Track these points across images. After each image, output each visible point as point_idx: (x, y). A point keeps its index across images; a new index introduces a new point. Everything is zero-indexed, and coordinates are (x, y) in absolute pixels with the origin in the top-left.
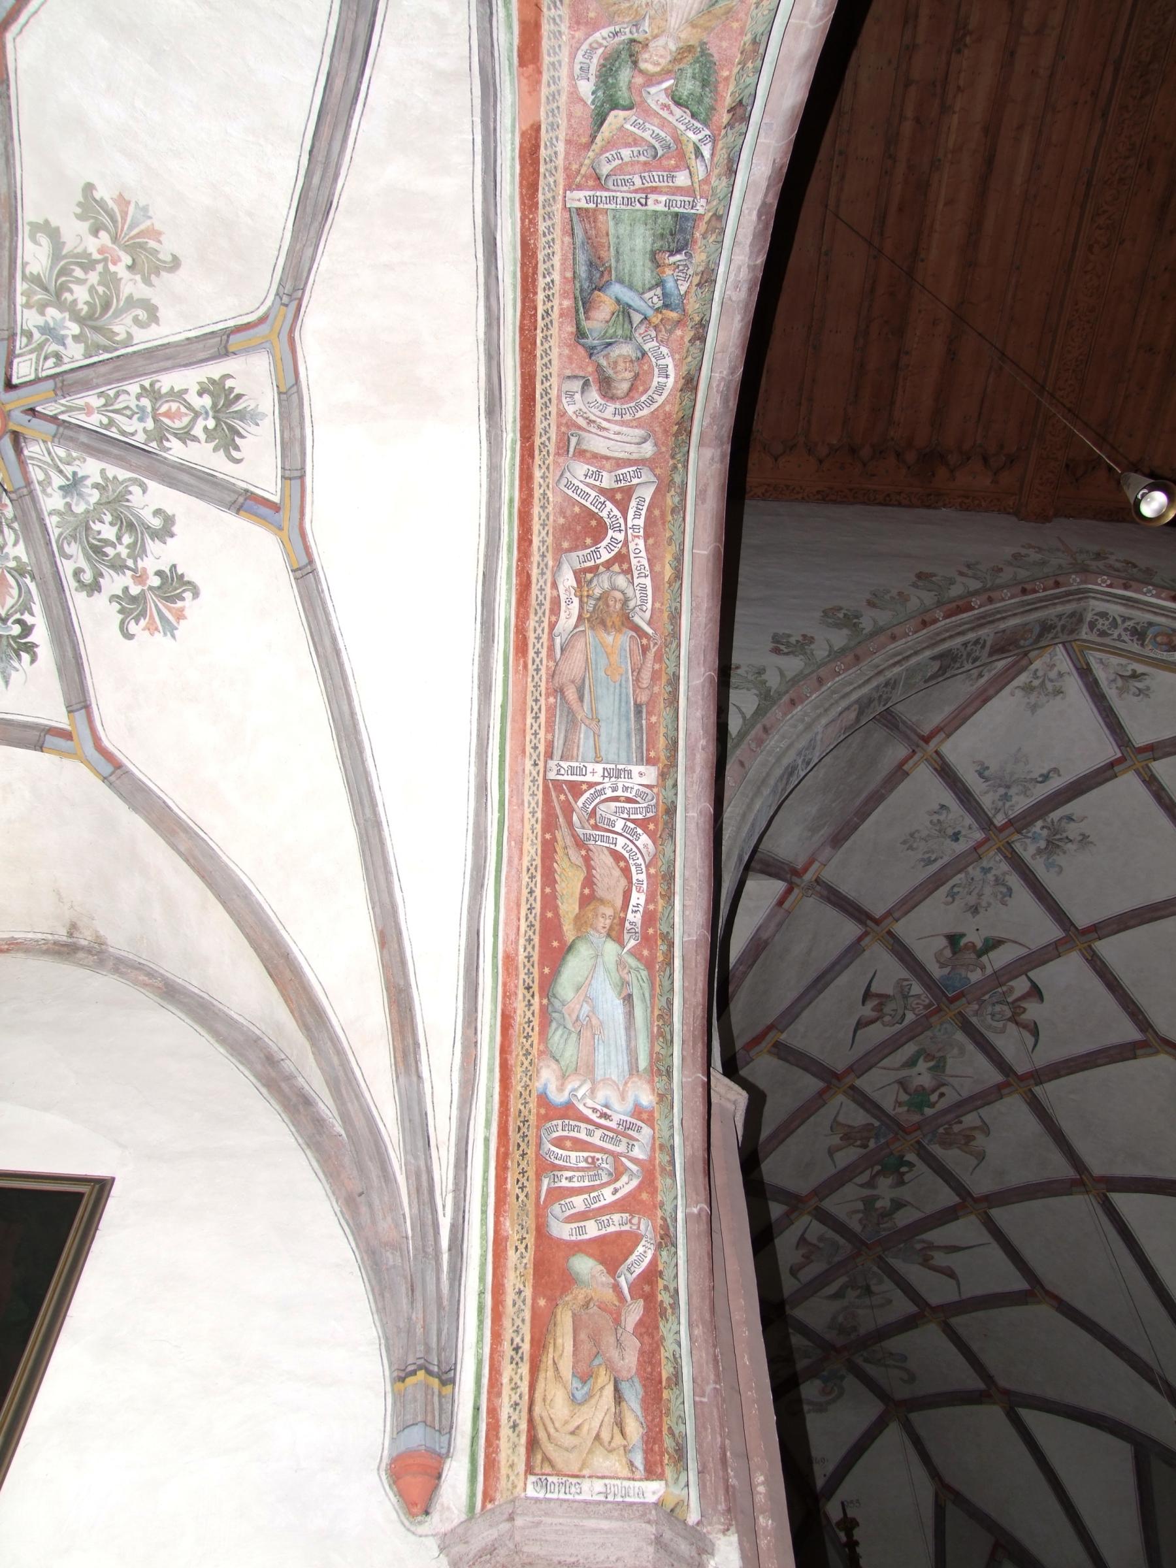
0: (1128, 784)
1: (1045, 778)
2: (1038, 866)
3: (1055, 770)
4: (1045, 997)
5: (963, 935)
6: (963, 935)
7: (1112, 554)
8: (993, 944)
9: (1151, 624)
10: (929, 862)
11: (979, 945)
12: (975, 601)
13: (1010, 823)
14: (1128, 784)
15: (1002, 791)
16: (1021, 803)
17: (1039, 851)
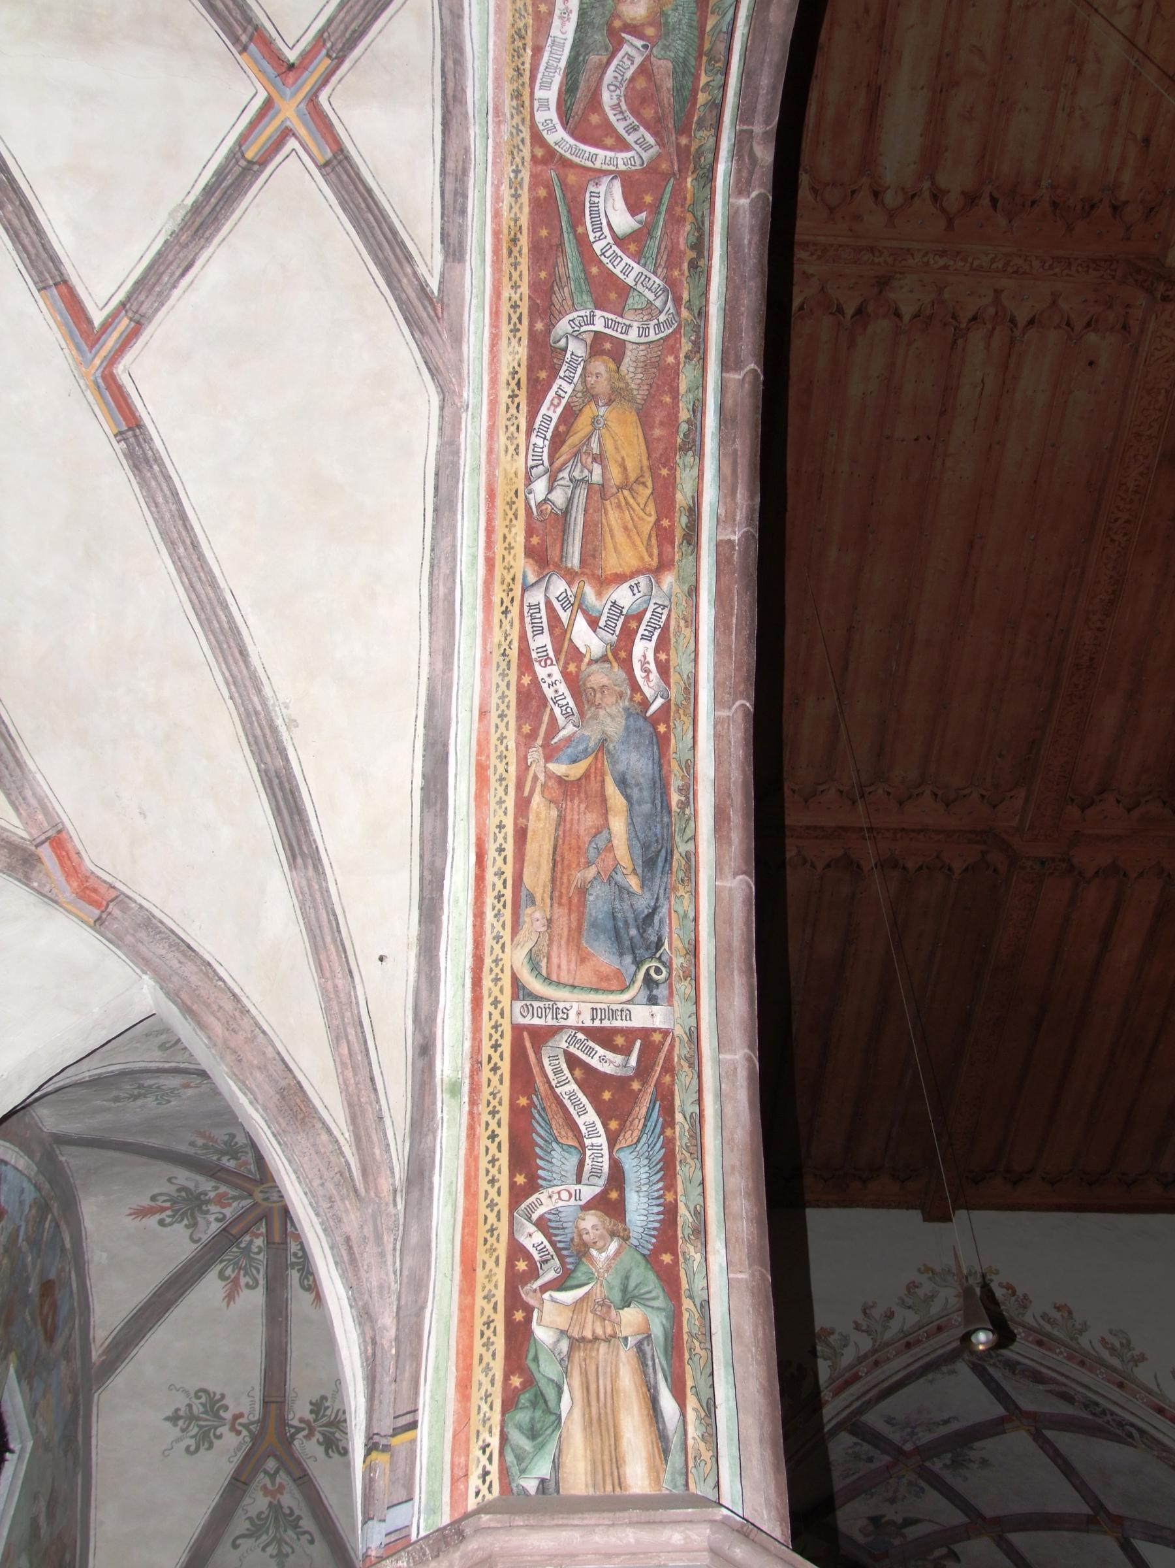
0: (1019, 1440)
1: (946, 1422)
2: (947, 1476)
3: (956, 1418)
4: (961, 1556)
5: (883, 1516)
6: (883, 1516)
7: (997, 1273)
8: (909, 1522)
9: (1018, 1363)
10: (848, 1476)
11: (900, 1521)
12: (862, 1369)
13: (918, 1450)
14: (1019, 1440)
15: (909, 1430)
16: (925, 1437)
17: (945, 1466)
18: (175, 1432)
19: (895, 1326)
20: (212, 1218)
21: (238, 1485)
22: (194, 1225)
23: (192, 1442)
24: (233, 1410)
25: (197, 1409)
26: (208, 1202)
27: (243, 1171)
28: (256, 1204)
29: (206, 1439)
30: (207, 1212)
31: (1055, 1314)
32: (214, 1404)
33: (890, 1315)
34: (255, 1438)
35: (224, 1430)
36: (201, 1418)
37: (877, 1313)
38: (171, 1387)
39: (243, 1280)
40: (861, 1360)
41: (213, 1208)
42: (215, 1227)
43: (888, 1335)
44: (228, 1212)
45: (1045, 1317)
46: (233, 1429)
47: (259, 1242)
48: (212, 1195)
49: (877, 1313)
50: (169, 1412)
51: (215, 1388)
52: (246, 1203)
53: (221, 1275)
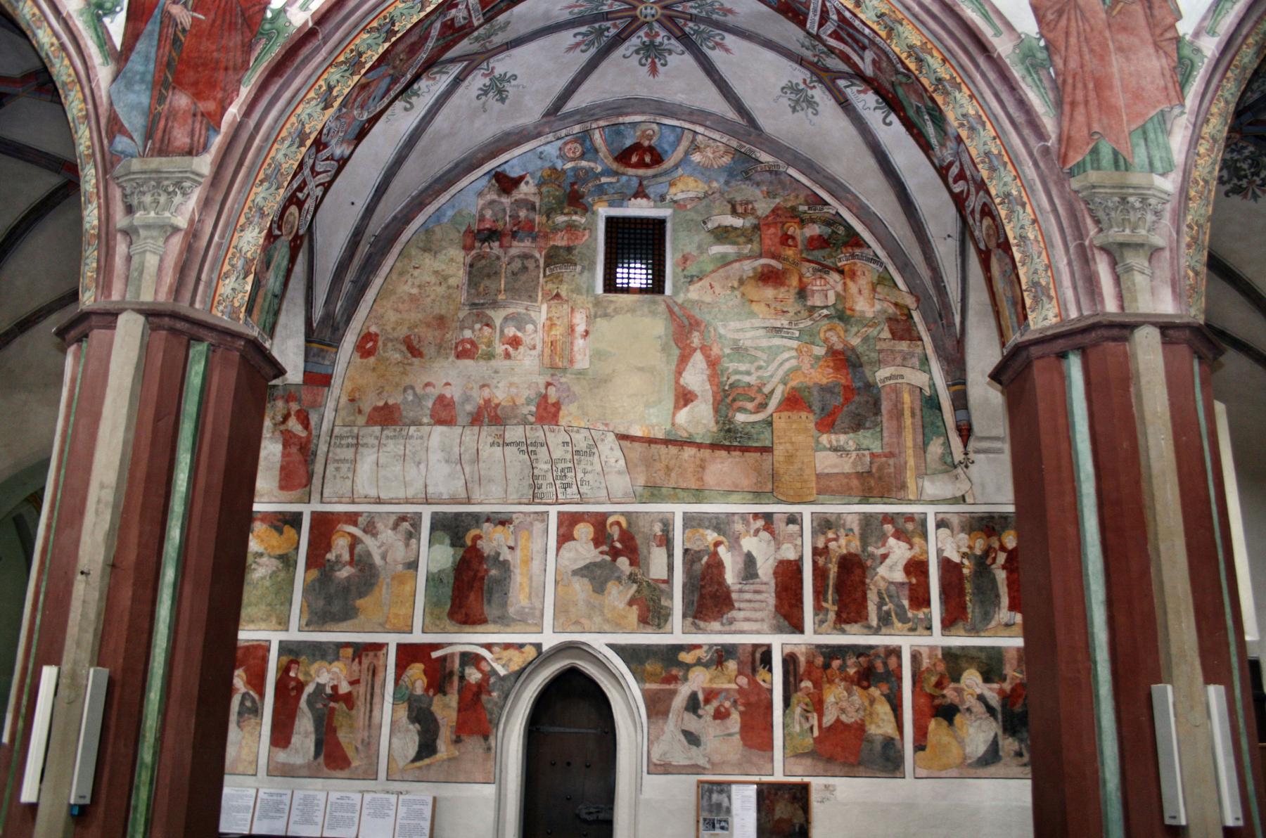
18: (801, 114)
20: (666, 42)
21: (845, 104)
22: (670, 52)
23: (810, 110)
24: (801, 82)
25: (793, 96)
26: (652, 42)
27: (622, 26)
28: (657, 21)
29: (811, 103)
30: (661, 44)
32: (792, 88)
34: (821, 81)
35: (810, 92)
36: (799, 99)
38: (776, 101)
39: (717, 39)
41: (658, 40)
42: (673, 41)
44: (663, 33)
46: (812, 88)
47: (691, 24)
48: (645, 39)
50: (790, 110)
51: (784, 83)
52: (656, 25)
53: (713, 48)
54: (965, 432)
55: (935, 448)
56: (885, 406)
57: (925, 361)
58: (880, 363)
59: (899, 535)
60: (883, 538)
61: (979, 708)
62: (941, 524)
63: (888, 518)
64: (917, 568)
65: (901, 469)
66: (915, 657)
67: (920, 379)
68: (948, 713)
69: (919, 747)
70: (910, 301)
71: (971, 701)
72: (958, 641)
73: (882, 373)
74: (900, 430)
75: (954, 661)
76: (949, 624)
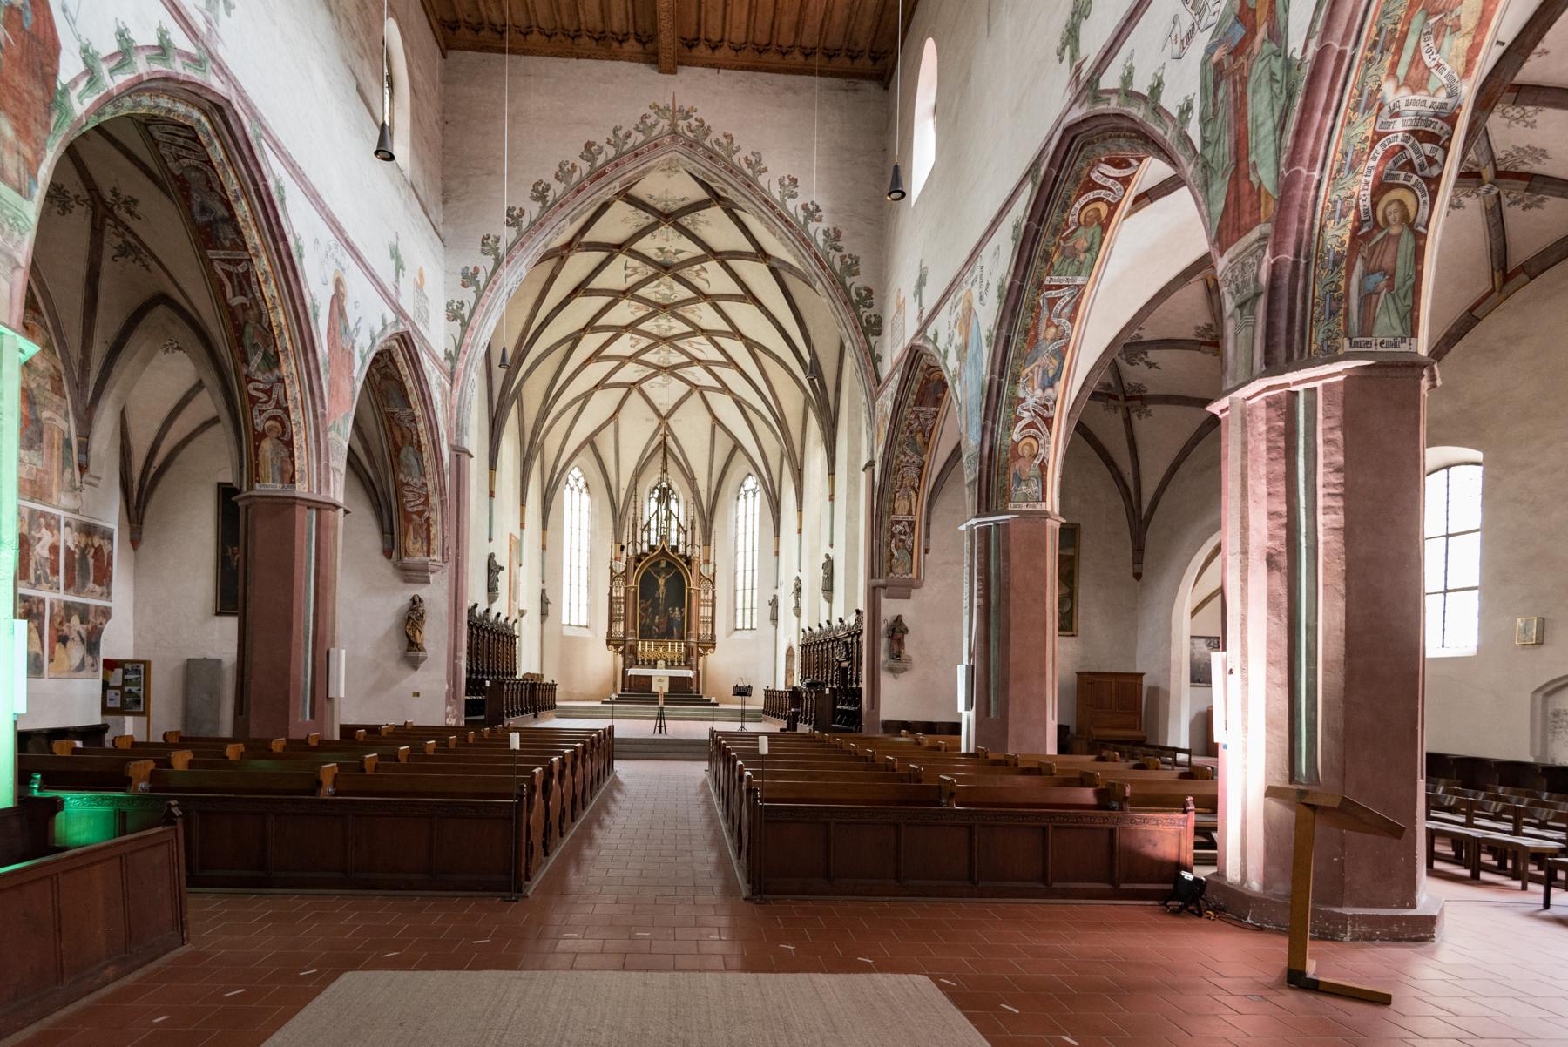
12: (608, 169)
19: (630, 142)
31: (723, 141)
33: (628, 136)
37: (621, 134)
40: (607, 163)
43: (626, 148)
45: (717, 142)
49: (621, 134)
54: (83, 468)
55: (67, 475)
56: (45, 437)
57: (67, 414)
58: (45, 406)
59: (48, 526)
60: (39, 527)
61: (78, 639)
62: (67, 525)
63: (43, 515)
64: (54, 549)
65: (50, 483)
66: (51, 605)
67: (62, 425)
68: (64, 640)
69: (51, 660)
70: (61, 367)
71: (74, 635)
72: (71, 598)
73: (46, 414)
74: (52, 456)
75: (69, 608)
76: (68, 587)
